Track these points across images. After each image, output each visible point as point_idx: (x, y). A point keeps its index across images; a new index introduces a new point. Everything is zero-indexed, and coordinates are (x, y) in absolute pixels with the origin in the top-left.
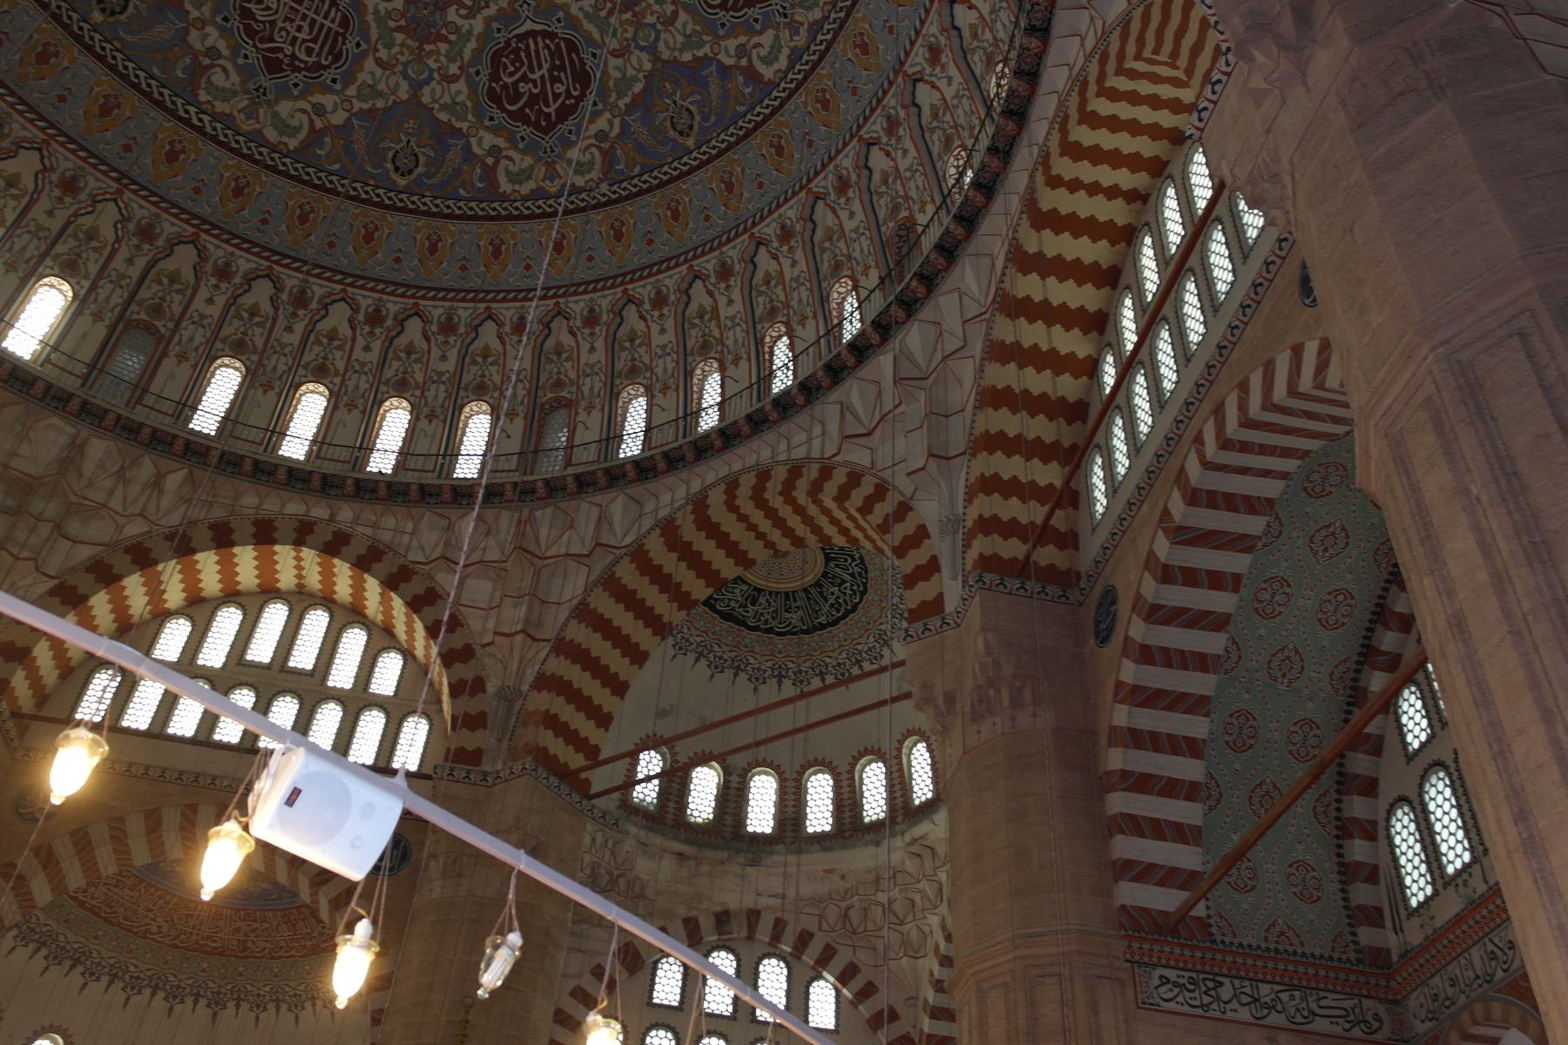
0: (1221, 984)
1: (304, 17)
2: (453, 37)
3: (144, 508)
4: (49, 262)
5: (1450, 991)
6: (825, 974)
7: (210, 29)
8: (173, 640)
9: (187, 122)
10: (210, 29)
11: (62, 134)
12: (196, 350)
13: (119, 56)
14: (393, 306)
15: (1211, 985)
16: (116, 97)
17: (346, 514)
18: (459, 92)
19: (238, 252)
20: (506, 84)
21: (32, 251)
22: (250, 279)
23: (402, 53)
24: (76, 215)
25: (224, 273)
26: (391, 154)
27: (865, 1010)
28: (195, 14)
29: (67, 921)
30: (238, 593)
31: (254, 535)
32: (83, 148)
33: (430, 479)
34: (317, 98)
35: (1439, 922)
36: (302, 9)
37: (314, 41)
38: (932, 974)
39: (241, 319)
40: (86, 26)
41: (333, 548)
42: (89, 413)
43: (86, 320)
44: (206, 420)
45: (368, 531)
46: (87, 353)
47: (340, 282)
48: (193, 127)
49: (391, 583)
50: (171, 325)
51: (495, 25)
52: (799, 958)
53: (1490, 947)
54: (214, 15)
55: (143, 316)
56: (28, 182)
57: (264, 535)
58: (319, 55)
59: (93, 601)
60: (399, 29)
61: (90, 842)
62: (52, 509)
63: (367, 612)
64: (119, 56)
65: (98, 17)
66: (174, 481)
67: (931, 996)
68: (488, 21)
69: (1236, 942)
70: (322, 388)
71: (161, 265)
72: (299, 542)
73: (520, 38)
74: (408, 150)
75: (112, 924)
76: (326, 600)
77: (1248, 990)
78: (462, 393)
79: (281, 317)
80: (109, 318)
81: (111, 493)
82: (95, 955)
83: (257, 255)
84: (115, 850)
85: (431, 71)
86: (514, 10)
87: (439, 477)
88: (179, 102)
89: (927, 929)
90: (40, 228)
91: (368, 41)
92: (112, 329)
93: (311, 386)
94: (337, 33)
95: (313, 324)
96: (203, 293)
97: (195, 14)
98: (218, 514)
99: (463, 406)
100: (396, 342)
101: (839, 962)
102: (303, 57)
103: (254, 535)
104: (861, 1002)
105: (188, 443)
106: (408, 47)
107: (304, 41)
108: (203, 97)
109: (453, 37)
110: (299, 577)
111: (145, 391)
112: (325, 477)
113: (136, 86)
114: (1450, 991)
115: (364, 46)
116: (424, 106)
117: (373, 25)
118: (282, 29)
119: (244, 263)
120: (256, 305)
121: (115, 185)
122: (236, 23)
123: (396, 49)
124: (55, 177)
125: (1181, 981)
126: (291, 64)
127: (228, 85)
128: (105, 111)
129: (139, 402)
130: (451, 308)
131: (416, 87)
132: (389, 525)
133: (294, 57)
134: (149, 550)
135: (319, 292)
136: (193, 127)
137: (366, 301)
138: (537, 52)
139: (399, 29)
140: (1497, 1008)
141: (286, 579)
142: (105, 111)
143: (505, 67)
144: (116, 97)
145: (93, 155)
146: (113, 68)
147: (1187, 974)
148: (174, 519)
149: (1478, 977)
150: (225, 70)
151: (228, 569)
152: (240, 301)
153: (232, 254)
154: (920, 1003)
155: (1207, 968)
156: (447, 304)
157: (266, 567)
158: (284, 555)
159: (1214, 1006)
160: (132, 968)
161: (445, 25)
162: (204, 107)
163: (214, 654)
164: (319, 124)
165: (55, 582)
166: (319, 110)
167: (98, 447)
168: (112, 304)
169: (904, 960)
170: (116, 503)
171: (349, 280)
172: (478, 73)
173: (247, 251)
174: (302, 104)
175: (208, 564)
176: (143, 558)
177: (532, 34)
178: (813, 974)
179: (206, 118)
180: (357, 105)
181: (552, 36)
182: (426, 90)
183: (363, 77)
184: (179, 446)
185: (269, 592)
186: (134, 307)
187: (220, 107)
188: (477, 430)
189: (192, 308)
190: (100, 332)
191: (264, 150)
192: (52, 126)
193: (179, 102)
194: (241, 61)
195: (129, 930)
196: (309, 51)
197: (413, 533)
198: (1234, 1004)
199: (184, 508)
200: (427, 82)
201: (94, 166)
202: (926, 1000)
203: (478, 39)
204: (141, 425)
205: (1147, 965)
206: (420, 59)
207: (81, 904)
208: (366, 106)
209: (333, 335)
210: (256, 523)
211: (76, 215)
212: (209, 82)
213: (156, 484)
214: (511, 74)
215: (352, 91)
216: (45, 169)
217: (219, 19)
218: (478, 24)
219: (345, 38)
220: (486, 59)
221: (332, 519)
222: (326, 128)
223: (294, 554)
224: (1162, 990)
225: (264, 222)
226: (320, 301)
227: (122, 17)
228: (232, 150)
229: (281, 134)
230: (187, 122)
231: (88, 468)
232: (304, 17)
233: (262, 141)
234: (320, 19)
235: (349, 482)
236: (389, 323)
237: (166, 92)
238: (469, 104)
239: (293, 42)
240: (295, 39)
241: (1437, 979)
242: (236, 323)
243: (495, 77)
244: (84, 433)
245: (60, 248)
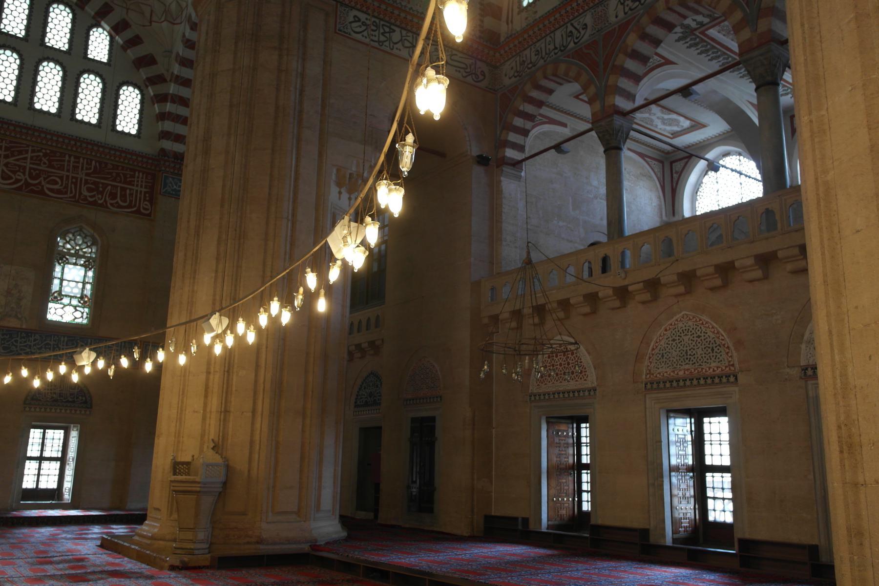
0: (394, 31)
5: (534, 58)
6: (103, 23)
15: (387, 30)
27: (132, 54)
35: (540, 14)
38: (184, 36)
52: (83, 8)
53: (570, 28)
67: (180, 49)
69: (409, 6)
77: (410, 39)
89: (184, 4)
101: (117, 15)
104: (129, 48)
114: (534, 58)
125: (368, 22)
140: (562, 67)
147: (373, 19)
149: (556, 48)
154: (174, 56)
155: (387, 19)
159: (387, 43)
169: (165, 24)
178: (94, 22)
198: (399, 45)
202: (178, 54)
205: (347, 6)
224: (354, 25)
241: (527, 52)
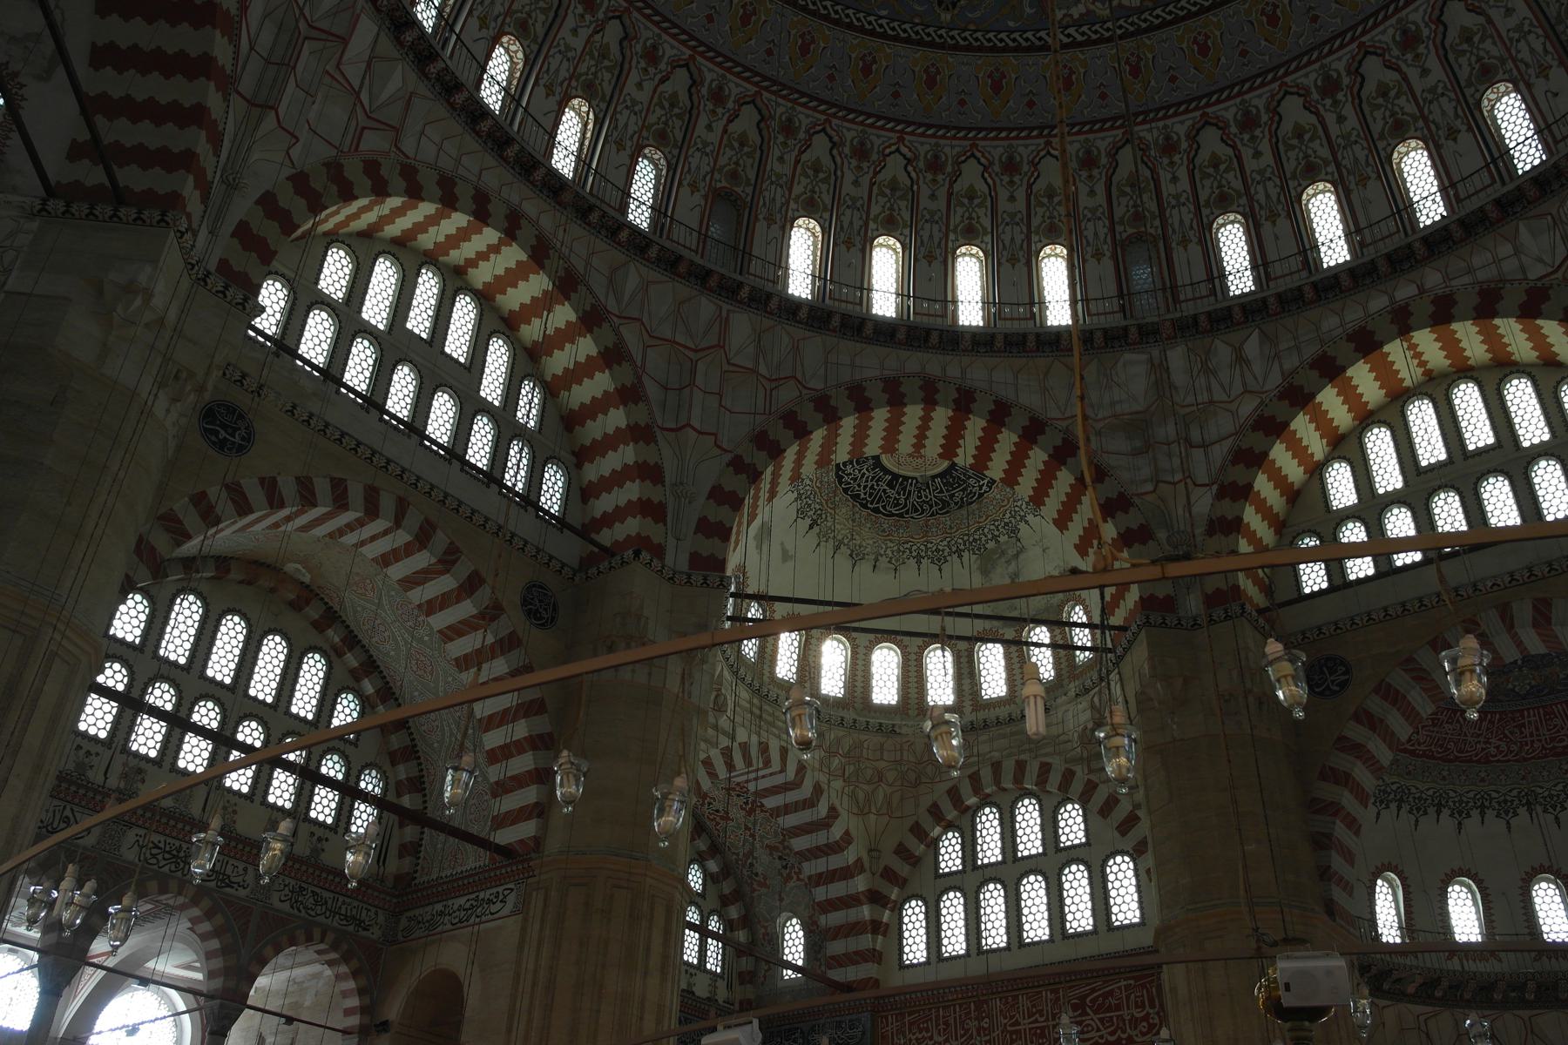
3: (1244, 384)
4: (1035, 238)
8: (1341, 487)
11: (980, 130)
12: (1192, 227)
13: (979, 35)
14: (1339, 63)
16: (997, 70)
17: (1433, 278)
19: (1169, 122)
21: (1019, 238)
22: (1193, 136)
24: (1030, 186)
25: (1169, 148)
29: (1409, 773)
30: (1371, 413)
31: (1356, 350)
32: (1001, 130)
33: (1499, 191)
39: (1209, 175)
40: (943, 32)
41: (1442, 314)
42: (1149, 334)
43: (1092, 262)
44: (1241, 281)
45: (1466, 279)
46: (1112, 289)
47: (1274, 80)
49: (1529, 311)
50: (1157, 222)
55: (1131, 231)
56: (981, 187)
57: (1367, 344)
59: (1257, 486)
61: (1397, 692)
62: (1169, 430)
63: (1516, 357)
64: (979, 35)
65: (946, 17)
66: (1252, 347)
70: (1321, 186)
71: (1115, 179)
72: (1404, 331)
75: (1450, 761)
76: (1465, 372)
78: (1468, 92)
79: (1243, 150)
80: (1107, 249)
81: (1209, 389)
82: (1452, 794)
83: (1187, 111)
84: (1424, 690)
87: (1504, 183)
90: (1012, 216)
92: (1115, 257)
93: (1310, 191)
95: (1274, 134)
96: (1165, 176)
98: (1311, 351)
99: (1479, 102)
100: (1364, 94)
103: (1356, 350)
105: (1243, 307)
110: (1422, 364)
111: (1174, 287)
112: (1388, 257)
113: (1006, 49)
119: (1180, 127)
120: (1214, 155)
121: (1042, 141)
124: (997, 168)
128: (997, 87)
129: (1176, 300)
130: (1400, 21)
132: (1486, 260)
134: (1273, 418)
135: (1261, 103)
137: (1309, 78)
141: (1408, 372)
142: (997, 87)
144: (997, 70)
145: (1012, 130)
148: (1275, 380)
151: (1350, 395)
152: (1198, 161)
156: (1393, 21)
157: (1385, 373)
158: (1395, 350)
160: (1494, 795)
163: (1389, 477)
165: (1215, 487)
167: (1177, 357)
168: (1102, 237)
170: (1219, 395)
171: (1282, 71)
173: (1176, 114)
175: (1330, 399)
176: (1276, 428)
179: (1071, 31)
184: (1237, 314)
185: (1399, 398)
186: (1119, 228)
188: (1512, 118)
189: (1165, 194)
190: (1108, 263)
192: (970, 130)
195: (1470, 761)
197: (1517, 252)
199: (1276, 366)
204: (1195, 317)
207: (1413, 753)
209: (1299, 133)
210: (1350, 338)
211: (1030, 186)
213: (1240, 359)
216: (986, 169)
221: (1422, 291)
223: (1405, 345)
225: (1173, 79)
226: (1267, 109)
231: (1179, 378)
235: (1417, 245)
236: (1346, 81)
237: (1029, 35)
242: (1207, 183)
244: (1156, 353)
245: (1035, 222)
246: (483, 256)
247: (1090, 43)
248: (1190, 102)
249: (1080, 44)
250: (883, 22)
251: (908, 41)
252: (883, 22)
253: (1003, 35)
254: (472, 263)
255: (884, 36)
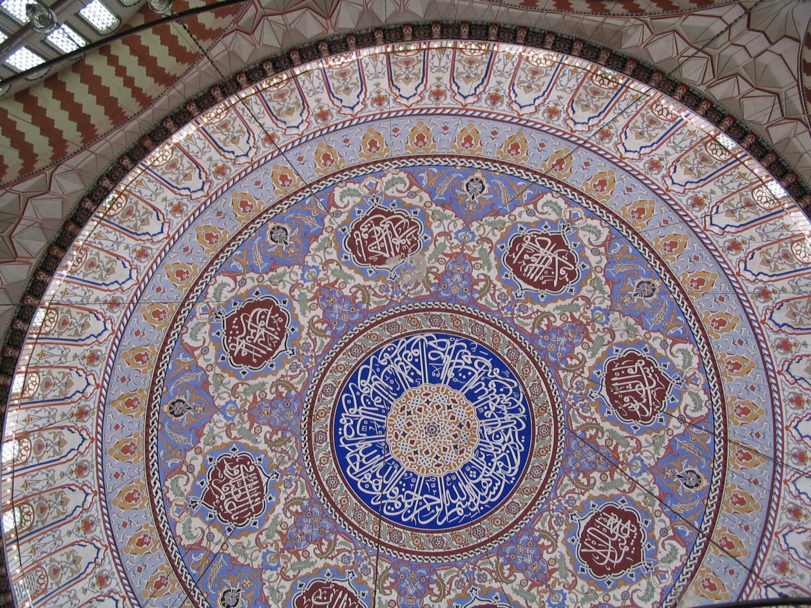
1: (243, 490)
2: (302, 559)
7: (200, 457)
9: (150, 488)
10: (200, 457)
13: (155, 432)
18: (283, 587)
19: (116, 575)
20: (310, 603)
23: (272, 545)
26: (226, 589)
28: (201, 445)
34: (214, 531)
36: (246, 486)
37: (238, 504)
48: (151, 492)
51: (328, 571)
54: (208, 453)
58: (234, 512)
60: (280, 533)
64: (155, 432)
65: (166, 408)
68: (326, 566)
71: (76, 547)
73: (336, 586)
74: (236, 594)
85: (279, 565)
86: (344, 571)
88: (157, 475)
91: (261, 525)
94: (250, 510)
97: (201, 445)
102: (226, 507)
106: (277, 545)
107: (233, 500)
108: (168, 483)
109: (302, 559)
113: (147, 451)
115: (257, 526)
116: (262, 579)
117: (270, 521)
118: (228, 486)
122: (213, 465)
123: (271, 541)
126: (218, 505)
127: (183, 488)
131: (265, 567)
133: (222, 502)
136: (151, 492)
138: (340, 600)
139: (280, 533)
143: (318, 594)
144: (136, 448)
146: (147, 435)
150: (188, 480)
153: (113, 574)
161: (304, 551)
162: (164, 488)
164: (204, 544)
166: (211, 537)
172: (301, 586)
174: (204, 526)
177: (345, 590)
180: (230, 551)
181: (354, 599)
182: (269, 572)
183: (244, 540)
187: (171, 495)
191: (170, 533)
193: (157, 475)
194: (198, 483)
196: (231, 507)
200: (272, 569)
201: (98, 470)
203: (314, 570)
206: (277, 556)
208: (233, 555)
212: (177, 479)
214: (318, 600)
215: (232, 542)
217: (208, 457)
218: (320, 563)
219: (252, 515)
220: (311, 582)
222: (205, 548)
227: (174, 418)
228: (156, 520)
229: (184, 533)
230: (150, 488)
232: (243, 490)
233: (172, 529)
234: (249, 497)
238: (284, 597)
239: (227, 497)
240: (230, 495)
243: (308, 594)
246: (121, 71)
247: (154, 507)
248: (130, 586)
249: (152, 501)
250: (165, 366)
251: (153, 384)
252: (165, 366)
253: (155, 448)
254: (113, 60)
255: (157, 367)
